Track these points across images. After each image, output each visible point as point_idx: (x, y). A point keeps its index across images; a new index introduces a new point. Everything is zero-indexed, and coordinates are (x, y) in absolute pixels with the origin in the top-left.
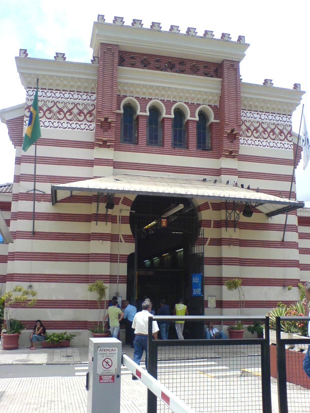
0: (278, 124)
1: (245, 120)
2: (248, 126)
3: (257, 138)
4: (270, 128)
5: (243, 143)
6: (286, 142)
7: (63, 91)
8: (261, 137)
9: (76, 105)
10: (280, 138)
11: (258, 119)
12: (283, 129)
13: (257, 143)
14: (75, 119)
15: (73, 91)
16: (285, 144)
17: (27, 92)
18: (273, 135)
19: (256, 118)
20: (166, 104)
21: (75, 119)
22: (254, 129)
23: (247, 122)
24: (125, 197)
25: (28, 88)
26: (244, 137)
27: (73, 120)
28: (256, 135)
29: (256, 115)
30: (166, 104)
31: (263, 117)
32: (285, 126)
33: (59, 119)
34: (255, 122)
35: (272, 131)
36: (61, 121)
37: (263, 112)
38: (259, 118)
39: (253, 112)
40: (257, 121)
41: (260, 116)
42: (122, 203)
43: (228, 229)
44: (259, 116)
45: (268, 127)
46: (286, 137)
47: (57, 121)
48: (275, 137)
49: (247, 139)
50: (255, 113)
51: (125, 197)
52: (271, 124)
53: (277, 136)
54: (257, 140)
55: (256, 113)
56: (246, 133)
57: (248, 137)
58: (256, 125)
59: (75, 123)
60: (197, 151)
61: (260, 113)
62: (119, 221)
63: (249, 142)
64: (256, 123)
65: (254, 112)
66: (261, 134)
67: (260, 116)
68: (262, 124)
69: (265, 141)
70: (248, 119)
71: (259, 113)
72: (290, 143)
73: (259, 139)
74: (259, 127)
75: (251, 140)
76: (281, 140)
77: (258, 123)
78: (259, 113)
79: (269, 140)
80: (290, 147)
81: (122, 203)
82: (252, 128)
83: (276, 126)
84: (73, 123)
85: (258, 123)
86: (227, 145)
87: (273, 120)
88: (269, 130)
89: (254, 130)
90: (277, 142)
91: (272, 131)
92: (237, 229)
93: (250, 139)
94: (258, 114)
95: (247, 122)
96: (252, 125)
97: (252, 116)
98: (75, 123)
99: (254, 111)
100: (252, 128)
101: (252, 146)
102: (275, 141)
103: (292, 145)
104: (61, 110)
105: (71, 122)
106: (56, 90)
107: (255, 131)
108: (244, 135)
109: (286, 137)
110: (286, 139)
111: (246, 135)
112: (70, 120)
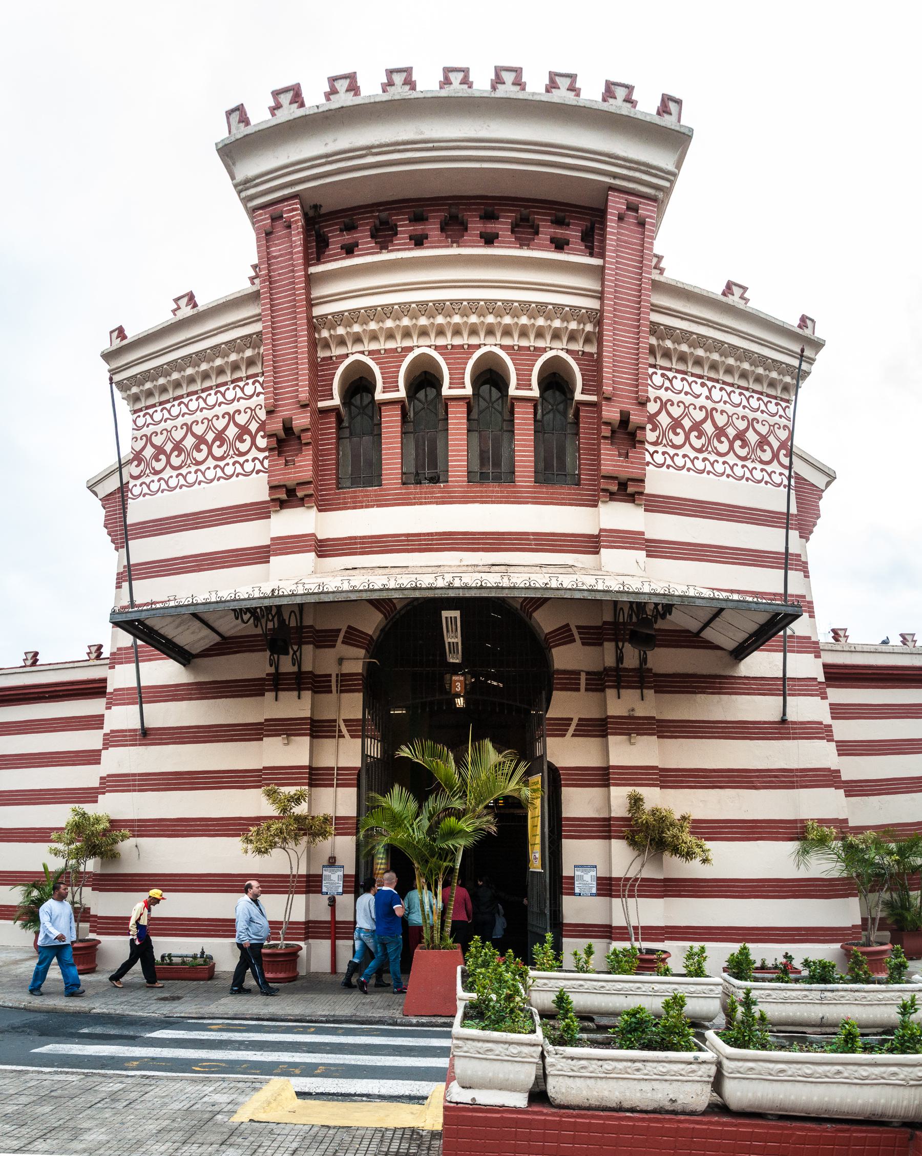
0: (753, 419)
1: (669, 400)
3: (700, 451)
4: (735, 428)
7: (203, 391)
8: (710, 449)
11: (702, 401)
17: (135, 422)
18: (742, 447)
24: (349, 627)
25: (135, 412)
28: (698, 443)
29: (697, 389)
34: (695, 408)
35: (741, 436)
36: (203, 468)
38: (707, 398)
39: (690, 379)
41: (710, 391)
42: (343, 642)
43: (623, 692)
44: (705, 391)
47: (193, 469)
48: (748, 454)
50: (696, 383)
51: (349, 627)
54: (701, 456)
55: (699, 381)
56: (671, 435)
57: (675, 447)
58: (699, 416)
59: (231, 461)
60: (535, 492)
61: (710, 384)
62: (337, 687)
66: (709, 442)
67: (710, 391)
68: (714, 412)
69: (721, 460)
70: (676, 398)
71: (707, 382)
73: (705, 455)
74: (704, 421)
76: (762, 462)
77: (704, 409)
78: (707, 382)
81: (343, 642)
82: (687, 424)
83: (751, 423)
85: (704, 409)
87: (744, 407)
89: (692, 429)
90: (753, 465)
91: (741, 436)
92: (649, 693)
94: (703, 385)
95: (672, 405)
96: (686, 414)
97: (687, 388)
98: (231, 461)
100: (687, 424)
102: (747, 463)
104: (201, 440)
105: (222, 464)
106: (188, 395)
107: (696, 433)
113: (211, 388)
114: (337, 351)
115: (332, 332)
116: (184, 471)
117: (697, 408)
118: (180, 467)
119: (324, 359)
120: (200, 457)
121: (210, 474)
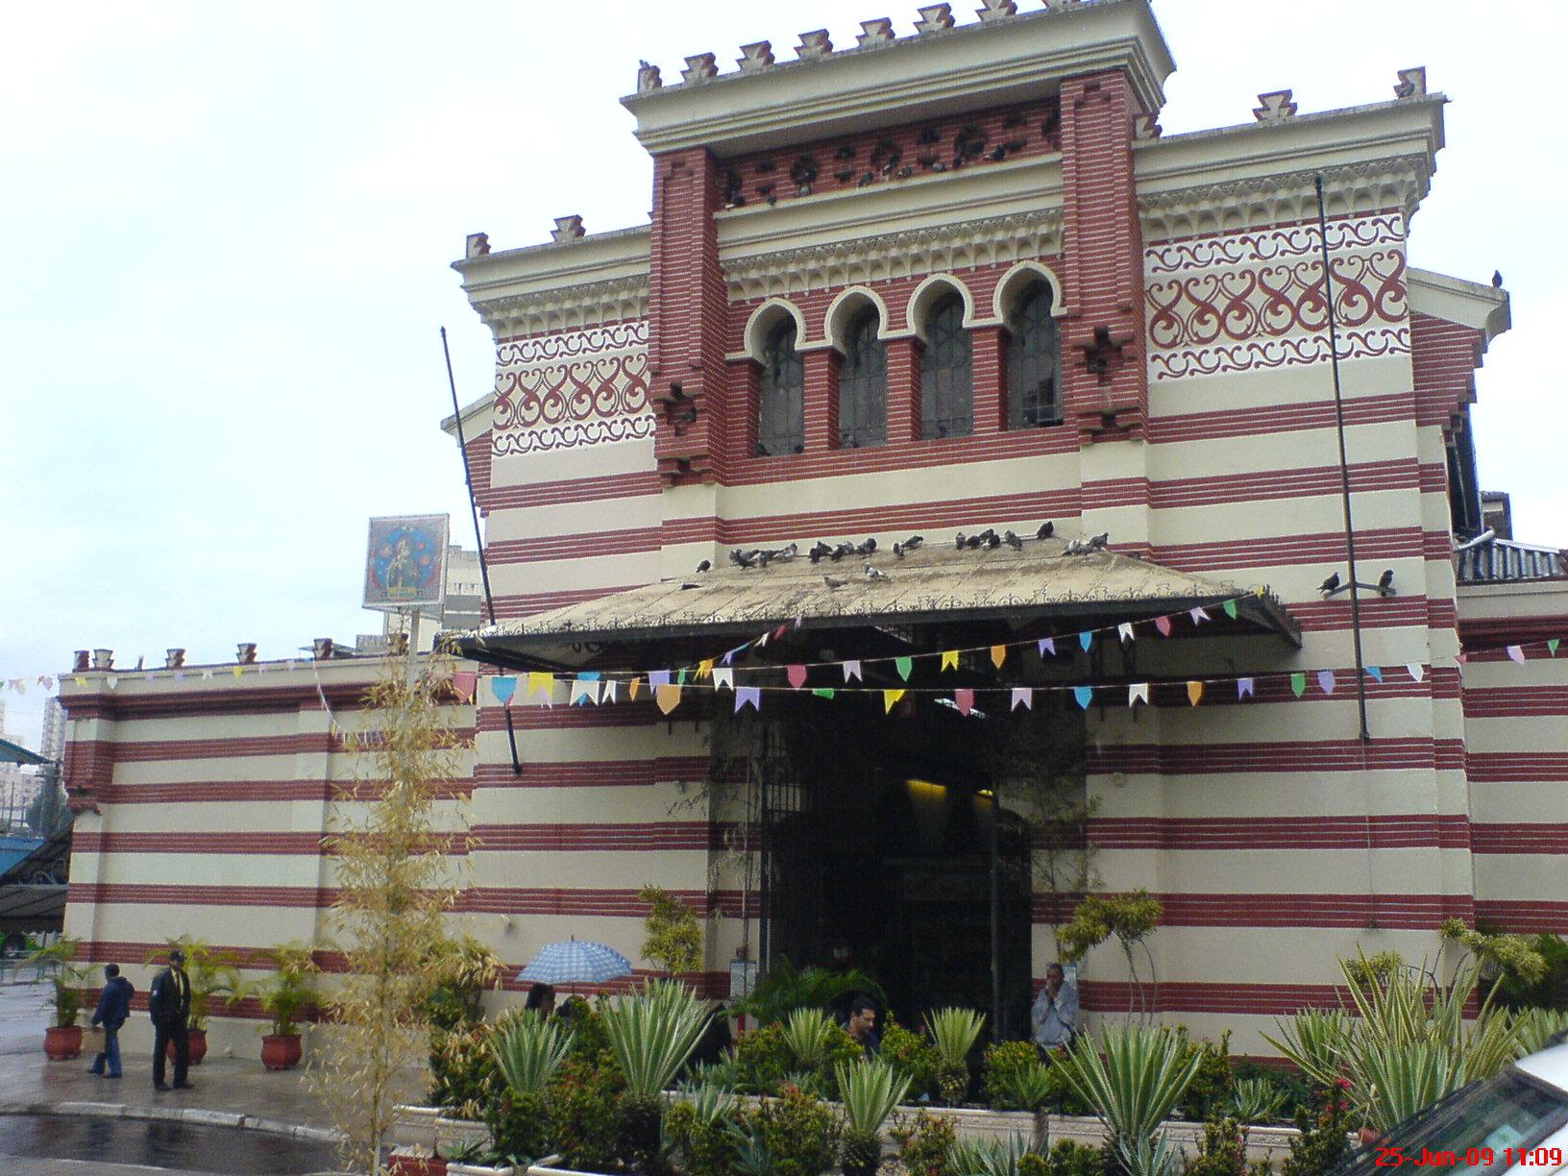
3: (1244, 336)
5: (1184, 368)
6: (1376, 324)
7: (588, 327)
9: (621, 365)
10: (1346, 317)
11: (1245, 262)
12: (1361, 275)
13: (1242, 357)
14: (620, 407)
15: (614, 323)
16: (1373, 333)
19: (1238, 259)
20: (887, 295)
21: (620, 407)
22: (1229, 305)
23: (1161, 289)
26: (1187, 344)
27: (616, 410)
29: (1234, 250)
30: (887, 295)
31: (1267, 247)
32: (1371, 260)
33: (579, 417)
36: (585, 423)
37: (1267, 228)
38: (1252, 256)
40: (1169, 280)
41: (1256, 245)
44: (1250, 248)
45: (1294, 280)
46: (1375, 305)
47: (573, 424)
49: (1197, 350)
50: (1233, 242)
63: (1210, 360)
64: (1165, 288)
65: (1229, 238)
67: (1256, 245)
71: (1250, 235)
72: (1396, 327)
75: (1217, 351)
77: (1247, 276)
78: (1250, 235)
79: (1296, 334)
80: (1394, 343)
84: (615, 422)
93: (1211, 347)
94: (1244, 241)
97: (1219, 254)
99: (1226, 233)
101: (1223, 374)
103: (1403, 334)
110: (1375, 312)
111: (1196, 334)
112: (609, 414)
113: (596, 326)
114: (747, 296)
115: (744, 276)
116: (561, 426)
117: (1237, 277)
118: (556, 420)
119: (735, 303)
120: (582, 409)
121: (594, 433)
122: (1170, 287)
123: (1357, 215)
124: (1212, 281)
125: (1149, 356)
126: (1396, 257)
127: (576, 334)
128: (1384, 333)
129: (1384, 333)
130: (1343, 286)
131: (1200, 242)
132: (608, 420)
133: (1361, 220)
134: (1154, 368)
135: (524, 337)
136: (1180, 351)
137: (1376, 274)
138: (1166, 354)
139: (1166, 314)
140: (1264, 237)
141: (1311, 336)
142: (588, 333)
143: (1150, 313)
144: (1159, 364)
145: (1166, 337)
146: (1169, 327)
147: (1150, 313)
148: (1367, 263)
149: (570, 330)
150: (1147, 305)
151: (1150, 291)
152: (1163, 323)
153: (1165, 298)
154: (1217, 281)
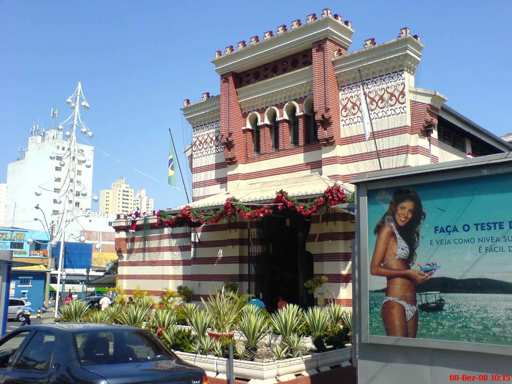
2: (354, 102)
12: (394, 91)
32: (396, 86)
46: (397, 100)
52: (379, 90)
53: (387, 102)
75: (357, 117)
86: (322, 133)
88: (377, 98)
93: (356, 116)
108: (350, 114)
109: (397, 100)
110: (397, 102)
111: (352, 113)
122: (346, 99)
123: (393, 73)
124: (356, 96)
125: (341, 120)
126: (403, 85)
127: (210, 125)
128: (400, 108)
129: (400, 108)
130: (389, 95)
131: (353, 85)
132: (217, 148)
133: (394, 74)
134: (342, 123)
135: (198, 127)
136: (349, 117)
137: (398, 91)
138: (345, 119)
139: (345, 107)
140: (369, 82)
141: (381, 110)
142: (212, 124)
143: (341, 107)
144: (343, 123)
145: (344, 114)
146: (345, 111)
147: (341, 107)
148: (395, 87)
149: (208, 124)
150: (340, 105)
151: (341, 101)
152: (344, 110)
153: (344, 103)
154: (357, 96)
